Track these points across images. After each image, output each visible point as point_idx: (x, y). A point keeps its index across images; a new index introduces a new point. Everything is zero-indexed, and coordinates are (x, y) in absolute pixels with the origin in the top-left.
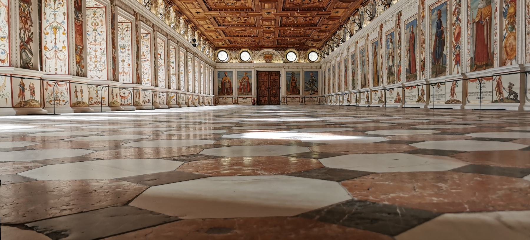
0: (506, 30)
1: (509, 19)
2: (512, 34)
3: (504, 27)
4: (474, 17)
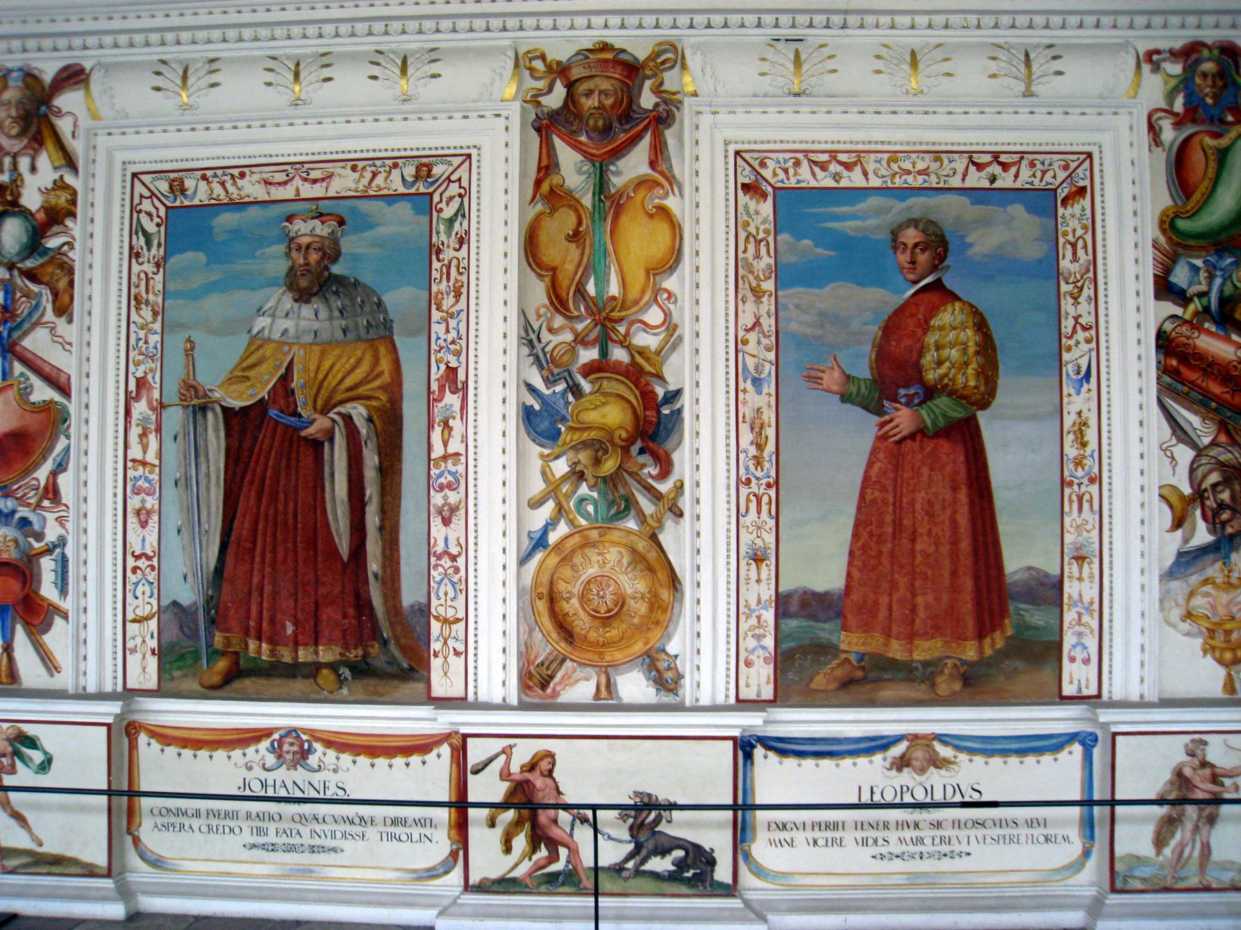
0: (550, 505)
1: (584, 457)
2: (615, 536)
3: (537, 486)
4: (210, 377)
